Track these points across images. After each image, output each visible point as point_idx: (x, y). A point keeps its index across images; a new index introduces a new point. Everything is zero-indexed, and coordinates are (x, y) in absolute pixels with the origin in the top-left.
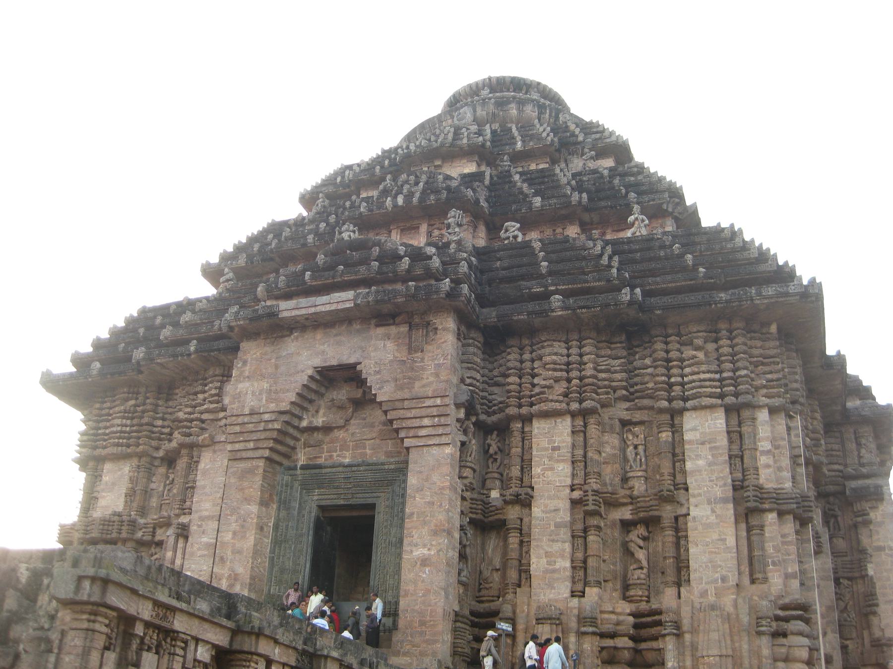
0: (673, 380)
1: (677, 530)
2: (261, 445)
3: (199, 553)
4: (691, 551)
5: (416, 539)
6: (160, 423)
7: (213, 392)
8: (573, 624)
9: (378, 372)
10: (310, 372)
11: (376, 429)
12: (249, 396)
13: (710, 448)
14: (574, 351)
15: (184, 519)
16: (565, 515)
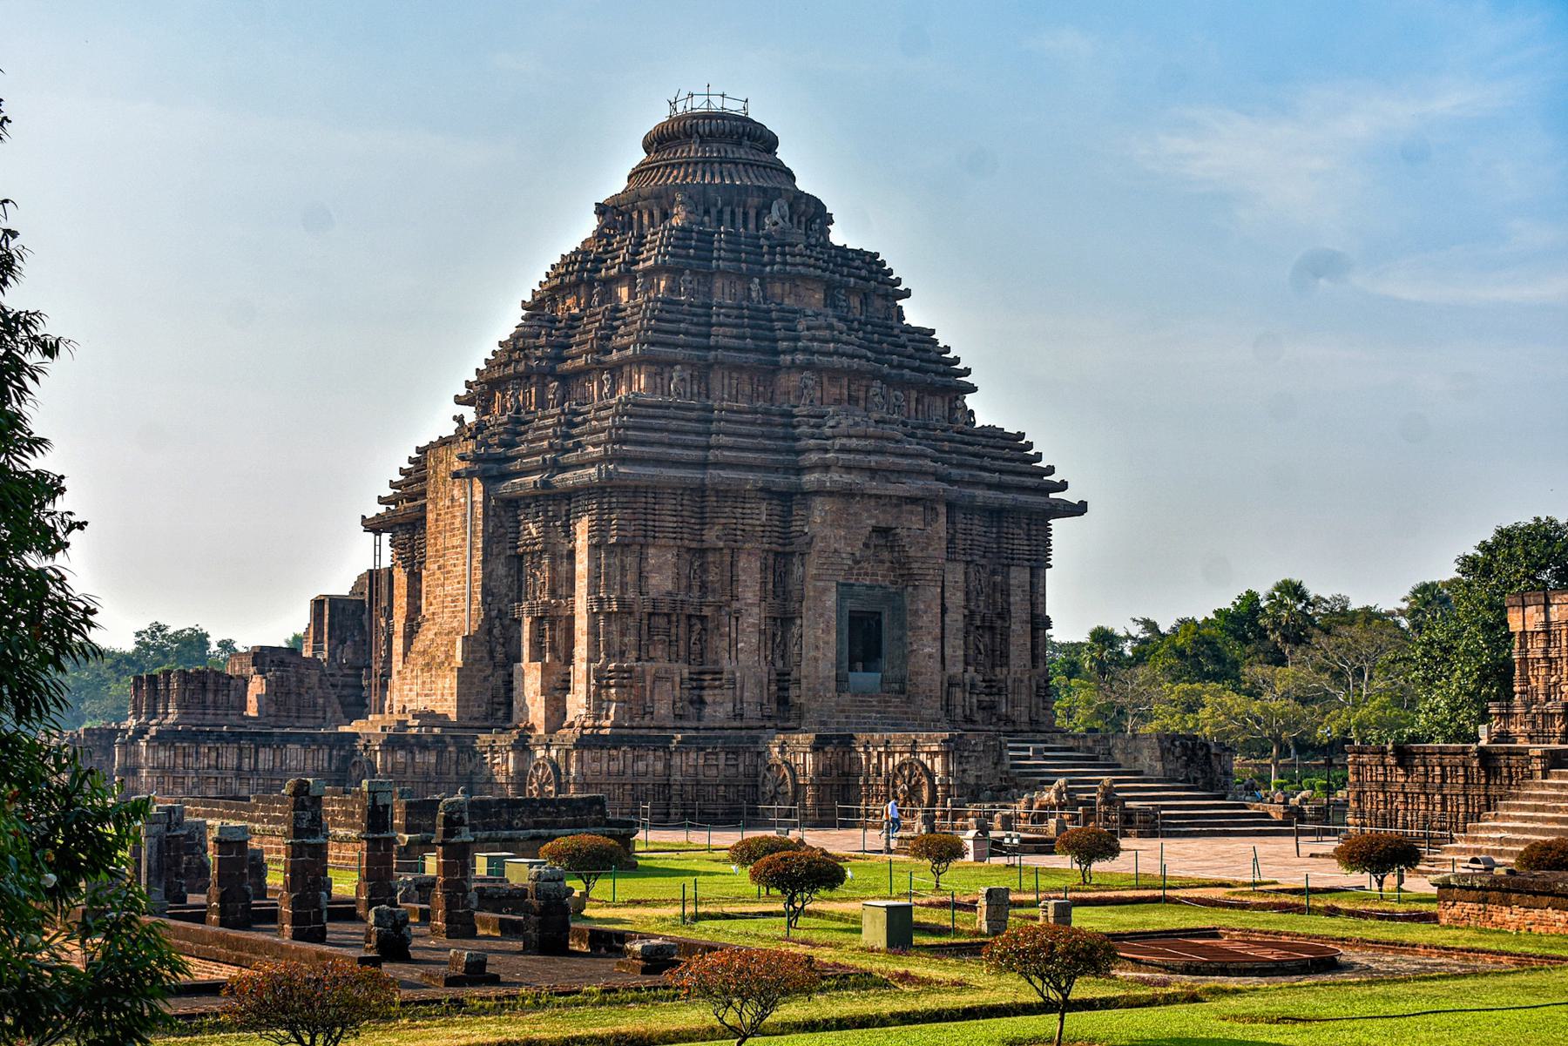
0: (1011, 547)
1: (1001, 635)
2: (836, 573)
3: (748, 630)
4: (1011, 648)
5: (925, 642)
6: (693, 521)
7: (757, 511)
8: (968, 688)
9: (909, 536)
10: (870, 529)
11: (887, 565)
12: (832, 541)
13: (1023, 591)
14: (969, 522)
15: (735, 605)
16: (961, 625)
